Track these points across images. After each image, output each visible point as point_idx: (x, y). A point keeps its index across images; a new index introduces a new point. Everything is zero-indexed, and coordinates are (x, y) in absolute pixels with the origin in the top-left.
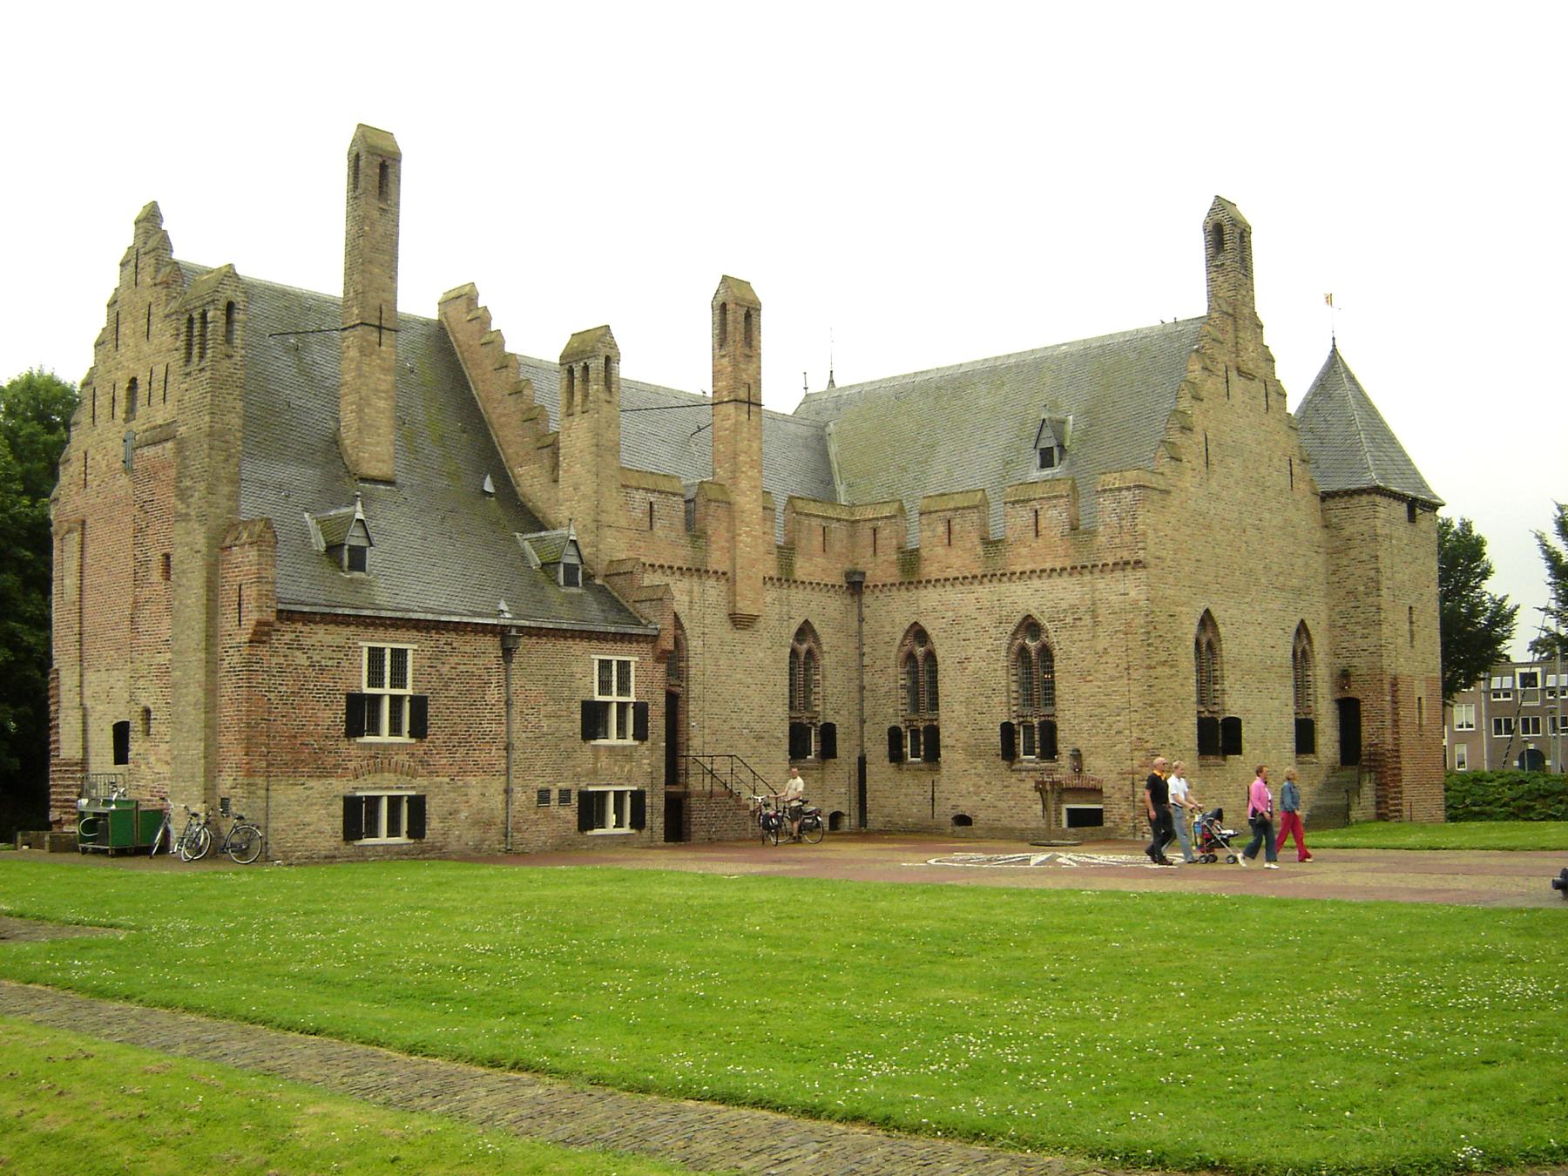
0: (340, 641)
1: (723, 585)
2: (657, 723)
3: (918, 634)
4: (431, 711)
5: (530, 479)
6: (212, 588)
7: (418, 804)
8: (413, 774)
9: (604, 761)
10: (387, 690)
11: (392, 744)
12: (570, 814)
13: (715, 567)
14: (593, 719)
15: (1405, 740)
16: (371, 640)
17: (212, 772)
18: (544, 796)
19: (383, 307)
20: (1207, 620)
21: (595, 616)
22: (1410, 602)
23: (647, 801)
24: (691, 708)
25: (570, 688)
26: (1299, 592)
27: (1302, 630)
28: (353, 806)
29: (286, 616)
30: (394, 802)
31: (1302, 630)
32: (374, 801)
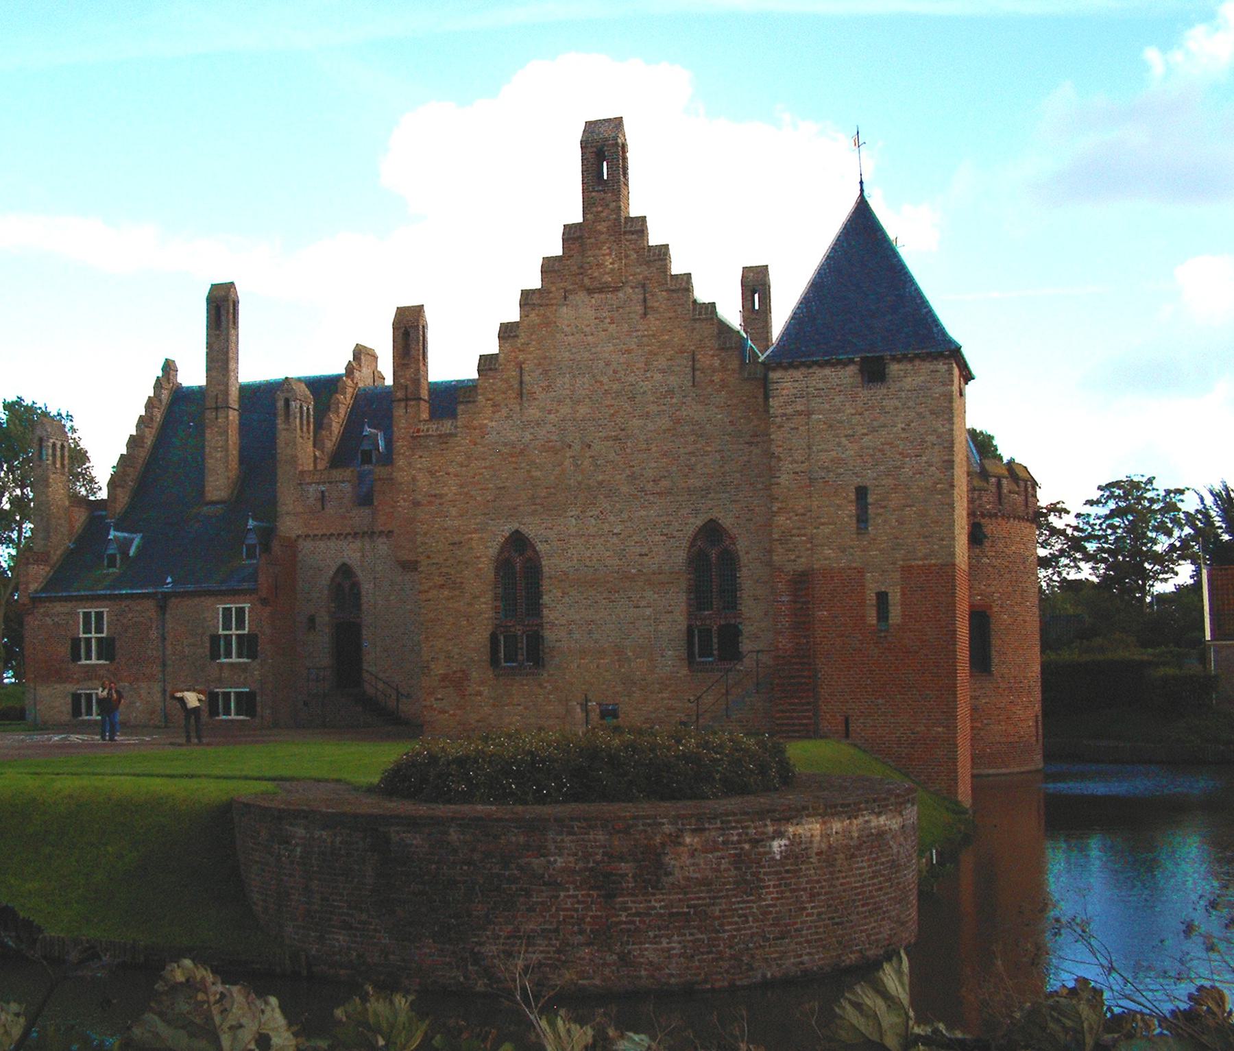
0: (66, 610)
4: (118, 644)
9: (226, 674)
11: (97, 664)
13: (381, 528)
16: (85, 608)
19: (219, 396)
20: (518, 541)
22: (858, 481)
23: (258, 698)
24: (364, 632)
25: (203, 628)
28: (76, 698)
31: (712, 531)
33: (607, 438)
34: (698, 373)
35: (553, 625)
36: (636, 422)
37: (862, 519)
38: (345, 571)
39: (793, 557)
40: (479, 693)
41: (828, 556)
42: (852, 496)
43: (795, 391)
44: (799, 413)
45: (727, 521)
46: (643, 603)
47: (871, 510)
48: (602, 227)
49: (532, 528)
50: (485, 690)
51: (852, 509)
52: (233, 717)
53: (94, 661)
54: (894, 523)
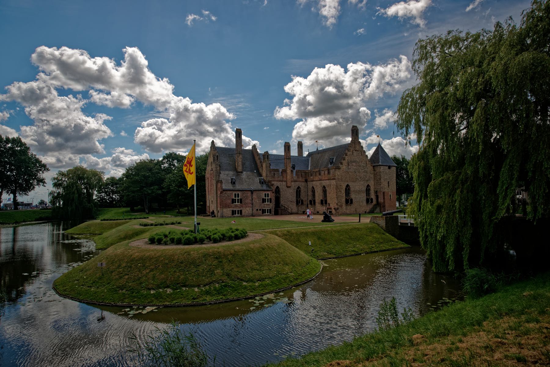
1: (285, 183)
3: (313, 187)
5: (261, 171)
6: (217, 187)
7: (241, 211)
10: (237, 198)
12: (261, 212)
14: (264, 201)
15: (386, 201)
17: (217, 208)
18: (257, 210)
20: (348, 186)
21: (265, 187)
26: (367, 181)
27: (368, 186)
28: (233, 211)
29: (224, 190)
30: (238, 211)
31: (368, 186)
32: (236, 211)
38: (278, 187)
41: (386, 190)
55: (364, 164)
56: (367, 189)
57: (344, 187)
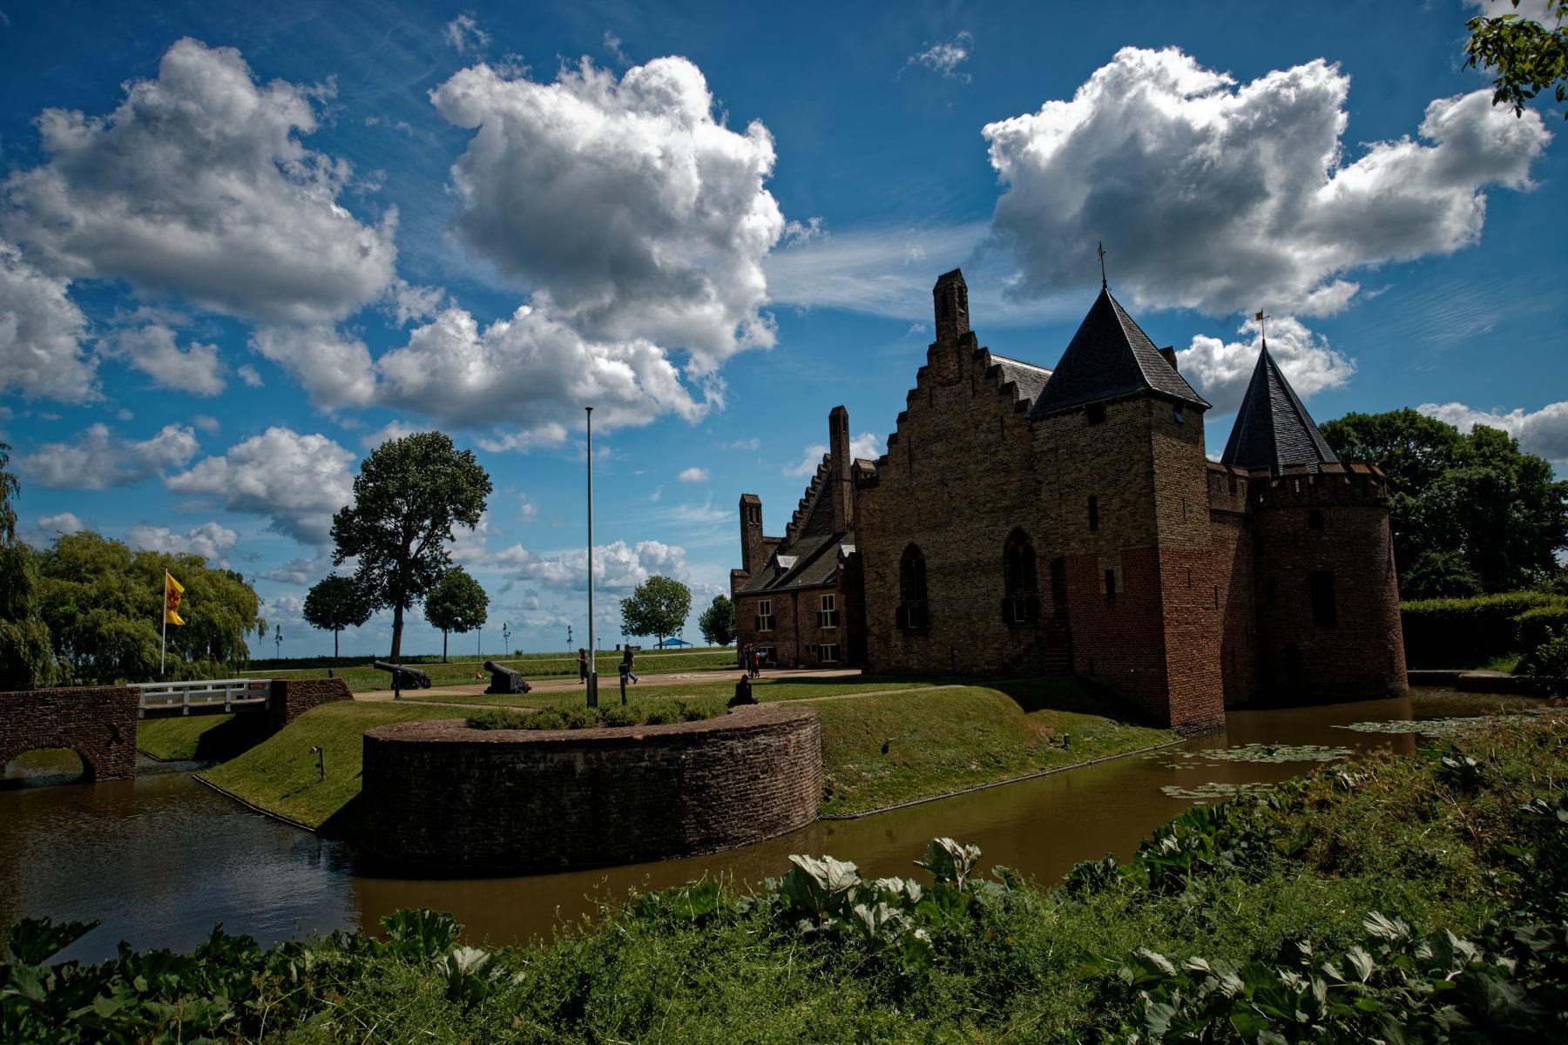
2: (843, 618)
8: (773, 641)
20: (912, 551)
26: (1009, 510)
27: (1018, 536)
31: (1018, 536)
33: (956, 479)
34: (1005, 430)
35: (933, 601)
36: (973, 467)
37: (1094, 519)
39: (1051, 549)
40: (897, 646)
42: (1087, 505)
43: (1047, 435)
44: (1050, 449)
45: (1026, 527)
46: (980, 585)
47: (1100, 513)
48: (947, 343)
49: (920, 540)
50: (899, 643)
51: (1086, 513)
52: (830, 661)
53: (766, 630)
54: (1115, 520)
55: (989, 431)
56: (1010, 554)
57: (896, 558)
